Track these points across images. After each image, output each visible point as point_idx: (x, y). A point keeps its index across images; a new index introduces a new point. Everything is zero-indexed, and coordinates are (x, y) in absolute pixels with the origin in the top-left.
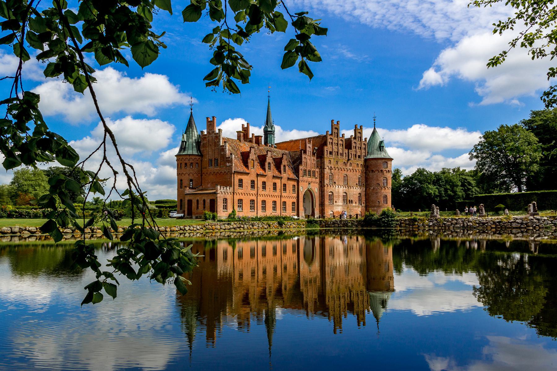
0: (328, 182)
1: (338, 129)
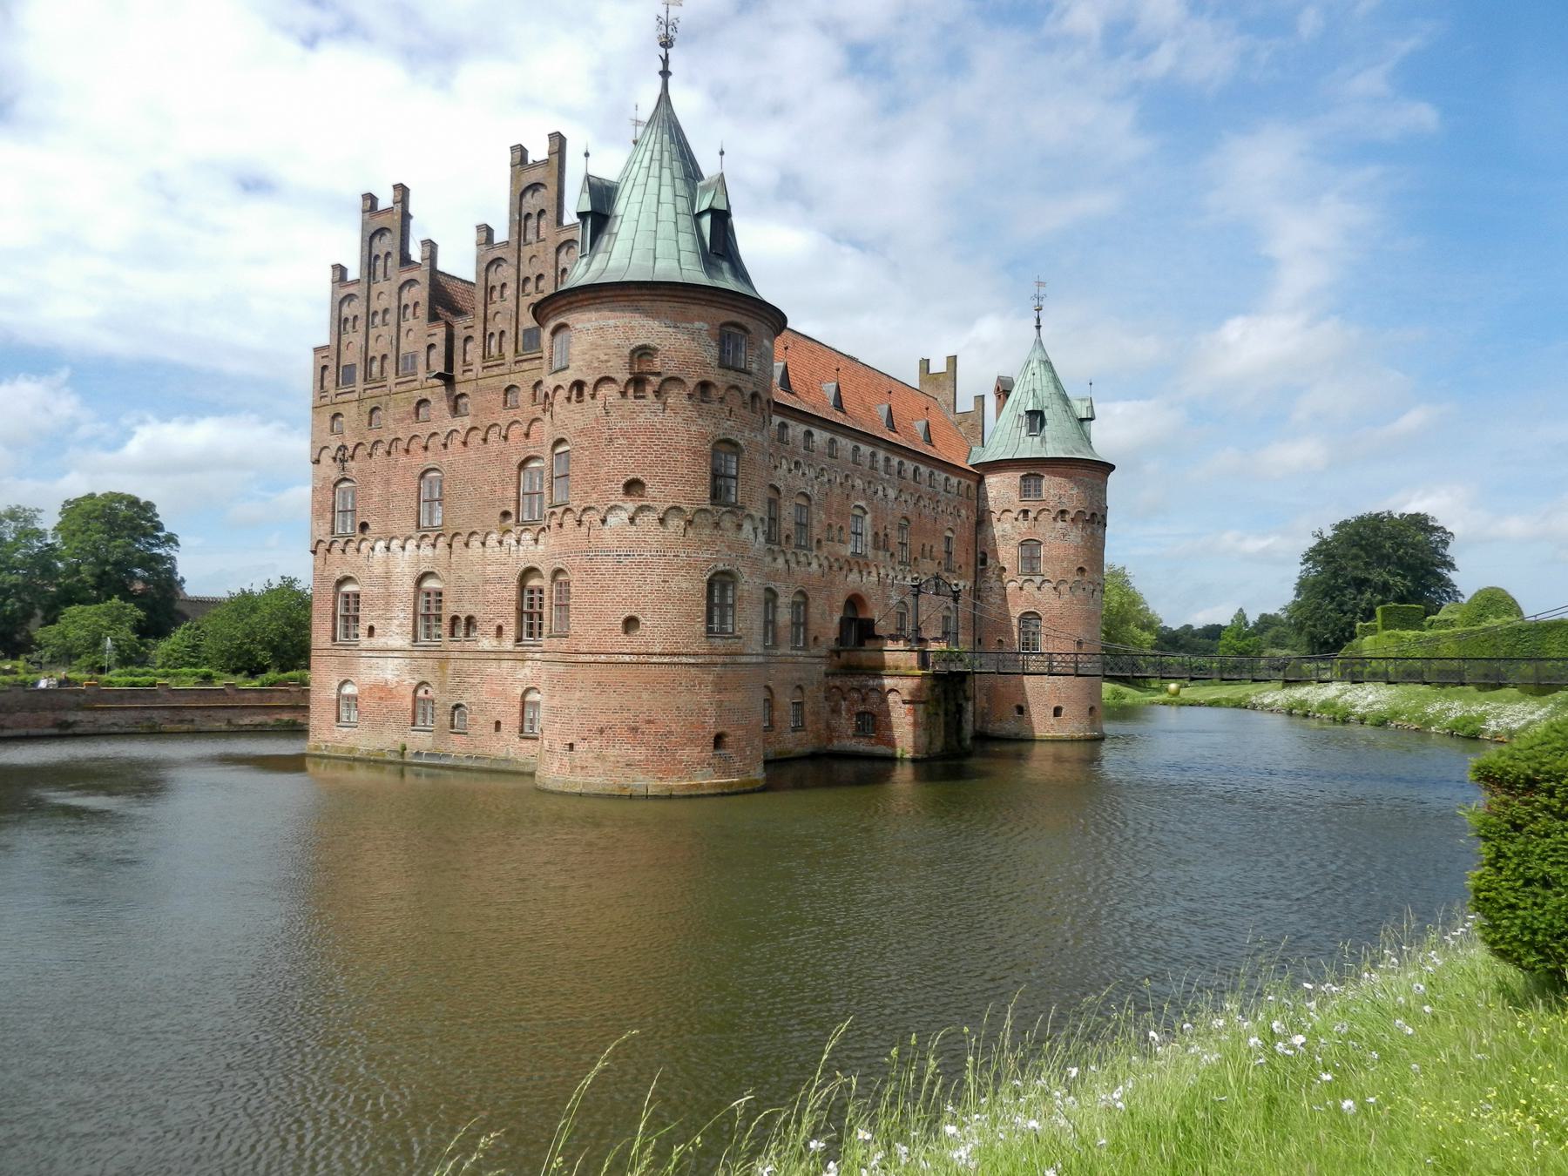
0: (328, 527)
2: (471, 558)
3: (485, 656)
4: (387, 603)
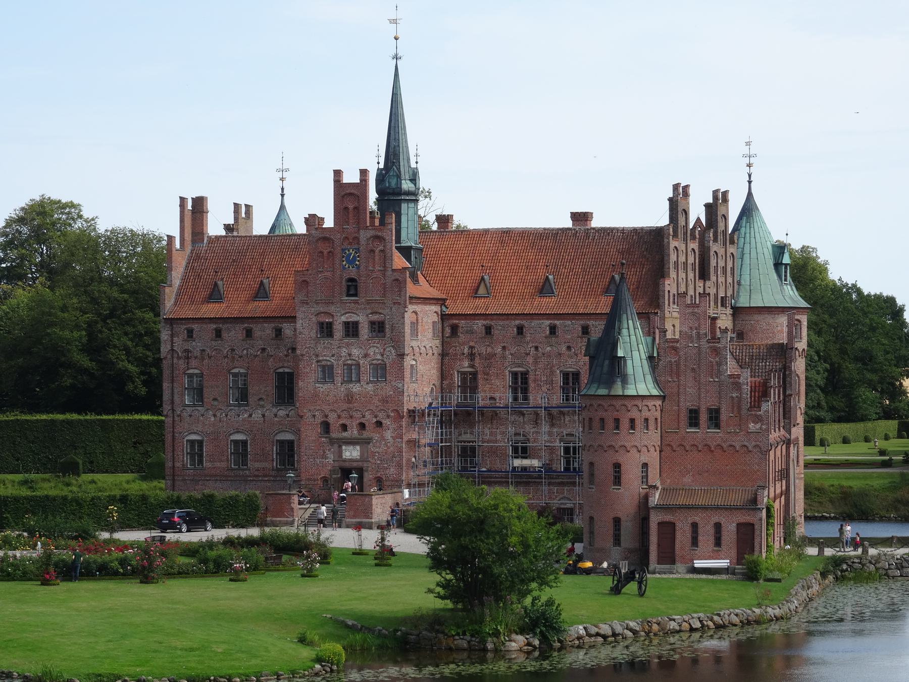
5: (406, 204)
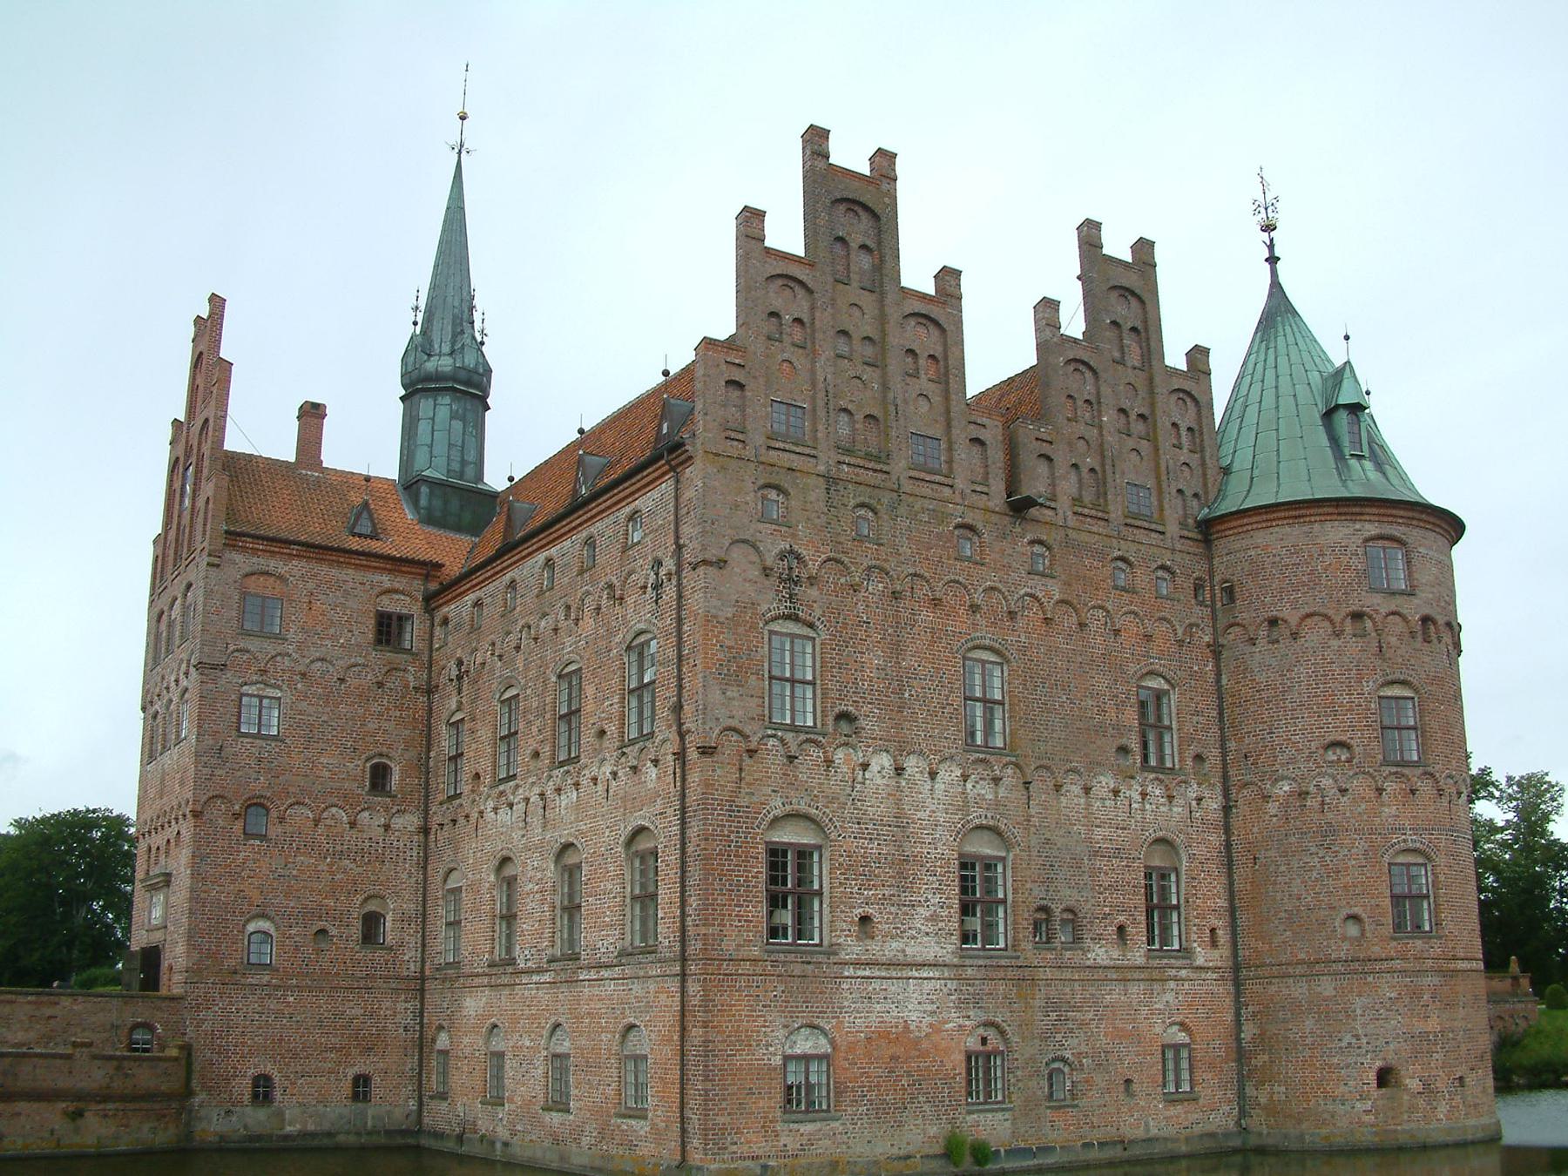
1: (875, 216)
2: (1064, 811)
3: (1101, 974)
4: (901, 874)
5: (431, 401)
